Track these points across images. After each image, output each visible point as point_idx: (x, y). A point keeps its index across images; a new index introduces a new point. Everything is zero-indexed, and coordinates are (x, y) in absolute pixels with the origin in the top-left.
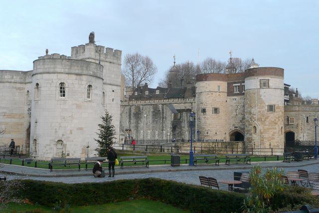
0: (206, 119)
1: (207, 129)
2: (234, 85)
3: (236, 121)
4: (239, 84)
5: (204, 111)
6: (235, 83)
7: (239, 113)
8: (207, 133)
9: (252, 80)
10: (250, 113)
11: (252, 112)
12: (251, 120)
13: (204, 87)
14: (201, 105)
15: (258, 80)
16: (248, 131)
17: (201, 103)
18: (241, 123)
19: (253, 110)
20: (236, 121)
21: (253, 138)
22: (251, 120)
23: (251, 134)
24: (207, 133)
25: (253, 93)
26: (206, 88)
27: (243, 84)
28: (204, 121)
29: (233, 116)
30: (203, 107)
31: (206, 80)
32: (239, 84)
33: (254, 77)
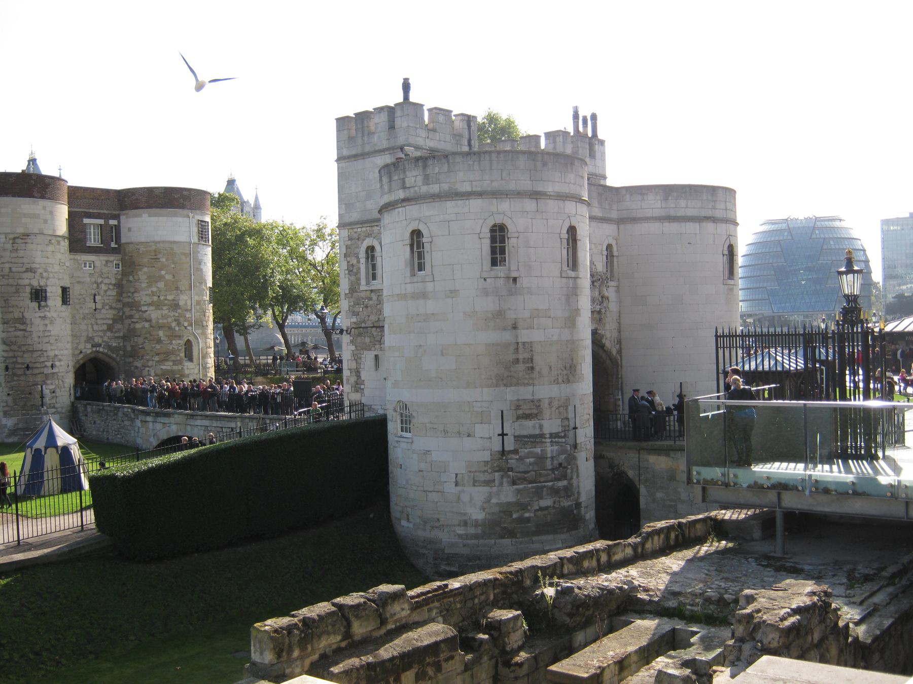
0: (47, 322)
1: (51, 354)
2: (86, 221)
3: (96, 328)
4: (101, 222)
5: (39, 295)
6: (90, 216)
7: (104, 305)
8: (52, 366)
9: (180, 219)
10: (175, 306)
11: (181, 303)
12: (179, 324)
13: (36, 216)
14: (29, 275)
15: (195, 221)
16: (166, 355)
17: (30, 270)
18: (109, 334)
19: (183, 299)
20: (96, 328)
21: (187, 372)
22: (179, 324)
23: (180, 362)
24: (52, 366)
25: (184, 254)
26: (46, 221)
27: (113, 222)
28: (42, 328)
29: (87, 311)
30: (35, 283)
31: (43, 197)
32: (101, 222)
33: (185, 212)
